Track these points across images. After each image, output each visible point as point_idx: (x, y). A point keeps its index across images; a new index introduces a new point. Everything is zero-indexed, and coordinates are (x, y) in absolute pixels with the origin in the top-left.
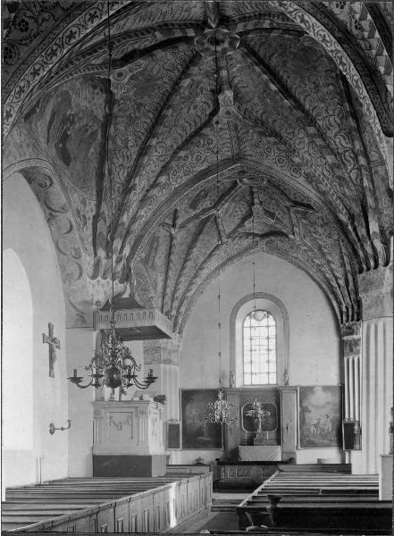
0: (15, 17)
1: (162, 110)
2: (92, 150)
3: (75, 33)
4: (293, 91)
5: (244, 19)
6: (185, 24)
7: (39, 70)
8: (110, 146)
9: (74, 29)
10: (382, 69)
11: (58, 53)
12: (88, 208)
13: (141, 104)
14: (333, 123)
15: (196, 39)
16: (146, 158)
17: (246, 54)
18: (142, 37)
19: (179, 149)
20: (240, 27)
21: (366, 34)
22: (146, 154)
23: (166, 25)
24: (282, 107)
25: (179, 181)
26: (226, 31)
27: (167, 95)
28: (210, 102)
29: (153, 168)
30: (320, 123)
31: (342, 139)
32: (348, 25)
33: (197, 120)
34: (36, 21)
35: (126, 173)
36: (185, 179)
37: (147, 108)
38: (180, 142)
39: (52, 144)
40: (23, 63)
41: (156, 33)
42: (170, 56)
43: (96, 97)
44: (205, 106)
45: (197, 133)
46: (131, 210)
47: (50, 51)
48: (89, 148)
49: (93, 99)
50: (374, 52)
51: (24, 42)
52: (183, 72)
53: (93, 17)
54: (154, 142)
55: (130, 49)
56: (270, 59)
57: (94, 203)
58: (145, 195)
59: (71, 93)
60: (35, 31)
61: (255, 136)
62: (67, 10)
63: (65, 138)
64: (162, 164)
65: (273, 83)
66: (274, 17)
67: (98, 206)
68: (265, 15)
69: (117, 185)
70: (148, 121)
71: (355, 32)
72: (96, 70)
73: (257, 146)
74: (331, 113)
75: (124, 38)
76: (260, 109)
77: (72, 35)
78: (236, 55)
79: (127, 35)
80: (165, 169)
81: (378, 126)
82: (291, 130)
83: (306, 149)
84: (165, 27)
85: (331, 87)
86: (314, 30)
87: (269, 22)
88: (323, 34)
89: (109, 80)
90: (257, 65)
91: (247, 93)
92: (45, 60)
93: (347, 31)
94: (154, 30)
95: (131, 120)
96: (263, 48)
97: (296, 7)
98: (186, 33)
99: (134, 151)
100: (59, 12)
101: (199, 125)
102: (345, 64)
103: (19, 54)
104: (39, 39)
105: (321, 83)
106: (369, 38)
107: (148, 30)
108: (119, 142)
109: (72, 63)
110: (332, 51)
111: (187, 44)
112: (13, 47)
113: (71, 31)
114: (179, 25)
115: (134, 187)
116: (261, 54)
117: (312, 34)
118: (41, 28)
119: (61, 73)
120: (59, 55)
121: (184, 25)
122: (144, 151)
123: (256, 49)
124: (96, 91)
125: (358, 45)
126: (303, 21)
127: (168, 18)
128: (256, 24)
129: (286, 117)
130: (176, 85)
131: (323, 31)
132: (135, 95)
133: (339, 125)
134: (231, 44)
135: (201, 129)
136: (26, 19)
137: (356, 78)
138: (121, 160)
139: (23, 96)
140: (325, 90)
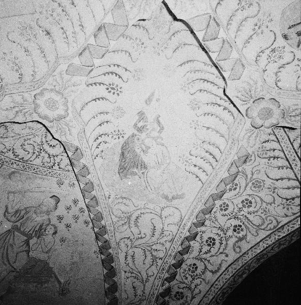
136: (181, 290)
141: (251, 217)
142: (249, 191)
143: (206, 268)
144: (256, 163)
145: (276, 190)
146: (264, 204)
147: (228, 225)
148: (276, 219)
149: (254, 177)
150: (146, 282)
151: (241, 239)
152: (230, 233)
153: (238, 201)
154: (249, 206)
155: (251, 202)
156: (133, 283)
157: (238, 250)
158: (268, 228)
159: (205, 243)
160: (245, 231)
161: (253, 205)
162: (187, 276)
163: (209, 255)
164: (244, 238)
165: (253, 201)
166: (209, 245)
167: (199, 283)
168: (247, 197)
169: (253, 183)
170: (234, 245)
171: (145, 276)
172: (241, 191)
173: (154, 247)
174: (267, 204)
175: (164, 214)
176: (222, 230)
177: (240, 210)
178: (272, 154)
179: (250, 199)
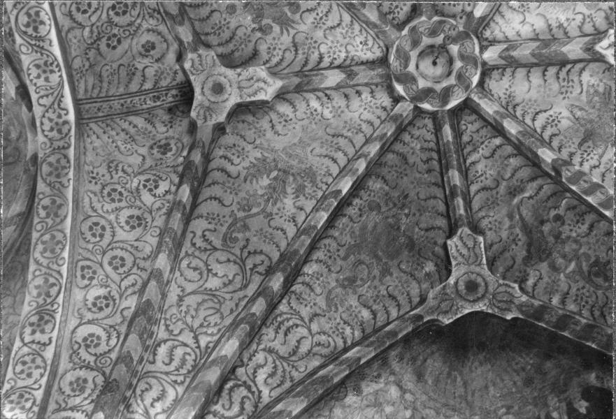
14: (293, 338)
28: (231, 46)
33: (204, 12)
44: (226, 35)
74: (315, 327)
82: (217, 243)
83: (190, 288)
85: (366, 314)
91: (261, 133)
133: (294, 352)
140: (353, 301)
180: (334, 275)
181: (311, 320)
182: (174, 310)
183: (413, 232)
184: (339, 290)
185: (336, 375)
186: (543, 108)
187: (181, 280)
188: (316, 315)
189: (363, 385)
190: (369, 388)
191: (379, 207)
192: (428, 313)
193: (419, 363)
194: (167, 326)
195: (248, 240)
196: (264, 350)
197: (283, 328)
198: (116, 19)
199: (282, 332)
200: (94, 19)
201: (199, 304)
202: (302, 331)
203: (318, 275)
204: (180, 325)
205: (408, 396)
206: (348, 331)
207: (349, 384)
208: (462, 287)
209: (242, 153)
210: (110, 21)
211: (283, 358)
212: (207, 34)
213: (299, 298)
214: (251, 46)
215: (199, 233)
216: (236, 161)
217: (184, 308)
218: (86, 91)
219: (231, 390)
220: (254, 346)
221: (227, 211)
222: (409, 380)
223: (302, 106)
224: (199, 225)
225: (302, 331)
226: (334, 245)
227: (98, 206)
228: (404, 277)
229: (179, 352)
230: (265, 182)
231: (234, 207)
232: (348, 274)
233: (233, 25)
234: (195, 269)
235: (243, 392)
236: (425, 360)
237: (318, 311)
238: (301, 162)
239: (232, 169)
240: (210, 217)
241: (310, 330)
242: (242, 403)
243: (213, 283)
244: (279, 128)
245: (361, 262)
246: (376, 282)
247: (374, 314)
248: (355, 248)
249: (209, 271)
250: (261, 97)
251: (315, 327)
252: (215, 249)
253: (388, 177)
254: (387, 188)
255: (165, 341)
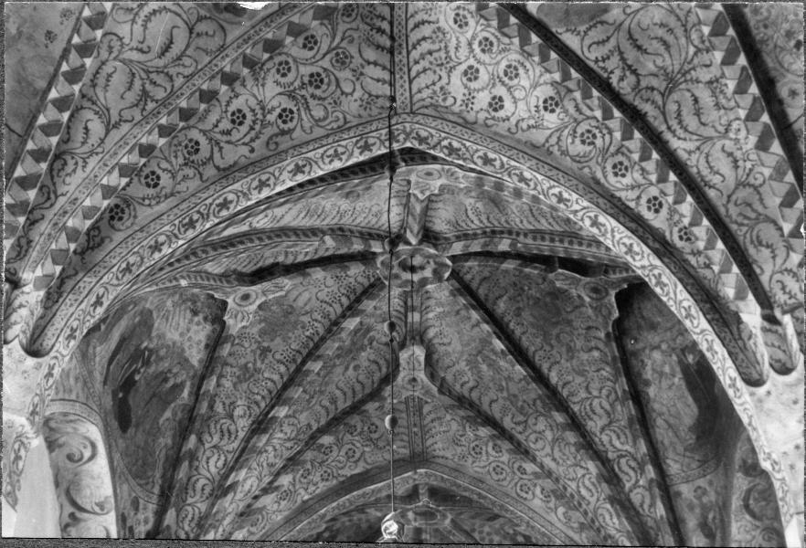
0: (144, 165)
1: (304, 362)
2: (168, 414)
3: (231, 202)
4: (530, 354)
5: (464, 236)
6: (370, 234)
7: (163, 244)
8: (203, 408)
9: (231, 197)
10: (729, 292)
11: (198, 225)
12: (141, 516)
13: (268, 350)
14: (598, 410)
15: (380, 259)
16: (264, 438)
17: (458, 290)
18: (303, 238)
19: (322, 431)
20: (457, 248)
21: (701, 245)
22: (265, 431)
23: (341, 229)
24: (509, 379)
25: (312, 488)
26: (432, 251)
27: (316, 339)
28: (382, 362)
29: (271, 460)
30: (576, 408)
31: (614, 437)
32: (667, 234)
33: (358, 387)
34: (174, 177)
35: (220, 464)
36: (322, 487)
37: (278, 356)
38: (323, 422)
39: (109, 389)
40: (141, 230)
41: (327, 238)
42: (330, 282)
43: (194, 328)
44: (374, 367)
45: (356, 408)
46: (221, 530)
47: (187, 220)
48: (164, 410)
49: (188, 330)
50: (716, 268)
51: (147, 202)
52: (350, 308)
53: (263, 184)
54: (281, 412)
55: (271, 261)
56: (495, 303)
57: (152, 507)
58: (249, 506)
59: (155, 315)
60: (168, 190)
61: (454, 426)
62: (224, 170)
63: (128, 384)
64: (287, 454)
65: (499, 338)
66: (518, 234)
67: (160, 514)
68: (502, 232)
69: (202, 482)
70: (276, 377)
71: (679, 244)
72: (212, 282)
73: (456, 442)
75: (278, 236)
76: (469, 378)
77: (225, 205)
78: (440, 293)
79: (283, 232)
80: (292, 462)
81: (733, 373)
82: (521, 418)
83: (548, 450)
84: (340, 232)
85: (596, 354)
86: (613, 237)
87: (509, 241)
88: (628, 242)
89: (225, 304)
90: (474, 308)
91: (447, 354)
92: (176, 231)
93: (667, 242)
94: (324, 233)
95: (247, 374)
96: (485, 285)
97: (586, 204)
98: (370, 246)
99: (243, 425)
100: (210, 172)
101: (360, 396)
102: (665, 285)
103: (135, 217)
104: (172, 201)
105: (578, 347)
106: (706, 248)
107: (314, 232)
108: (219, 408)
109: (194, 254)
110: (643, 267)
111: (364, 264)
112: (128, 206)
113: (225, 199)
114: (361, 233)
115: (233, 487)
116: (482, 292)
117: (609, 243)
118: (179, 188)
119: (177, 265)
120: (199, 228)
121: (368, 235)
122: (261, 425)
123: (474, 285)
124: (196, 319)
125: (686, 261)
126: (595, 223)
127: (347, 221)
128: (486, 245)
129: (515, 396)
130: (334, 326)
131: (629, 238)
132: (262, 333)
134: (435, 272)
135: (363, 402)
136: (159, 172)
137: (686, 304)
138: (216, 439)
139: (128, 277)
140: (585, 356)
141: (312, 102)
142: (326, 63)
143: (211, 157)
144: (354, 25)
145: (362, 78)
146: (339, 92)
147: (275, 103)
148: (345, 118)
149: (343, 45)
150: (114, 127)
151: (283, 133)
152: (272, 117)
153: (306, 71)
154: (318, 87)
155: (322, 81)
156: (174, 27)
157: (272, 147)
158: (329, 127)
159: (229, 114)
160: (295, 121)
161: (324, 87)
162: (179, 153)
163: (225, 138)
164: (290, 131)
165: (326, 80)
166: (233, 122)
167: (191, 175)
168: (321, 71)
169: (337, 54)
170: (271, 138)
171: (115, 118)
172: (317, 58)
173: (153, 76)
174: (343, 93)
175: (201, 27)
176: (263, 108)
177: (303, 86)
178: (378, 23)
179: (323, 75)
180: (563, 361)
181: (590, 393)
182: (561, 469)
183: (543, 290)
184: (574, 361)
185: (630, 410)
186: (463, 211)
187: (543, 453)
188: (587, 388)
189: (645, 377)
190: (648, 374)
191: (519, 309)
192: (606, 328)
193: (643, 323)
194: (569, 479)
195: (524, 401)
196: (601, 433)
197: (590, 413)
198: (359, 430)
199: (592, 416)
200: (358, 445)
201: (560, 451)
202: (596, 402)
203: (560, 375)
204: (571, 470)
205: (664, 346)
206: (604, 373)
207: (641, 387)
208: (594, 296)
209: (461, 373)
210: (360, 434)
211: (610, 423)
212: (373, 382)
213: (572, 394)
214: (382, 347)
215: (513, 426)
216: (466, 379)
217: (561, 462)
218: (404, 447)
219: (620, 468)
220: (597, 439)
221: (501, 401)
222: (653, 338)
223: (430, 323)
224: (507, 423)
225: (596, 402)
226: (541, 353)
227: (482, 464)
228: (577, 313)
229: (587, 483)
230: (484, 367)
231: (500, 395)
232: (564, 349)
233: (367, 364)
234: (537, 440)
235: (623, 461)
236: (643, 317)
237: (585, 385)
238: (475, 341)
239: (471, 384)
240: (504, 411)
241: (596, 397)
242: (630, 467)
243: (549, 435)
244: (445, 341)
245: (558, 336)
246: (576, 333)
247: (597, 349)
248: (546, 336)
249: (540, 433)
250: (422, 359)
251: (595, 393)
252: (526, 421)
253: (497, 294)
254: (505, 298)
255: (578, 487)
